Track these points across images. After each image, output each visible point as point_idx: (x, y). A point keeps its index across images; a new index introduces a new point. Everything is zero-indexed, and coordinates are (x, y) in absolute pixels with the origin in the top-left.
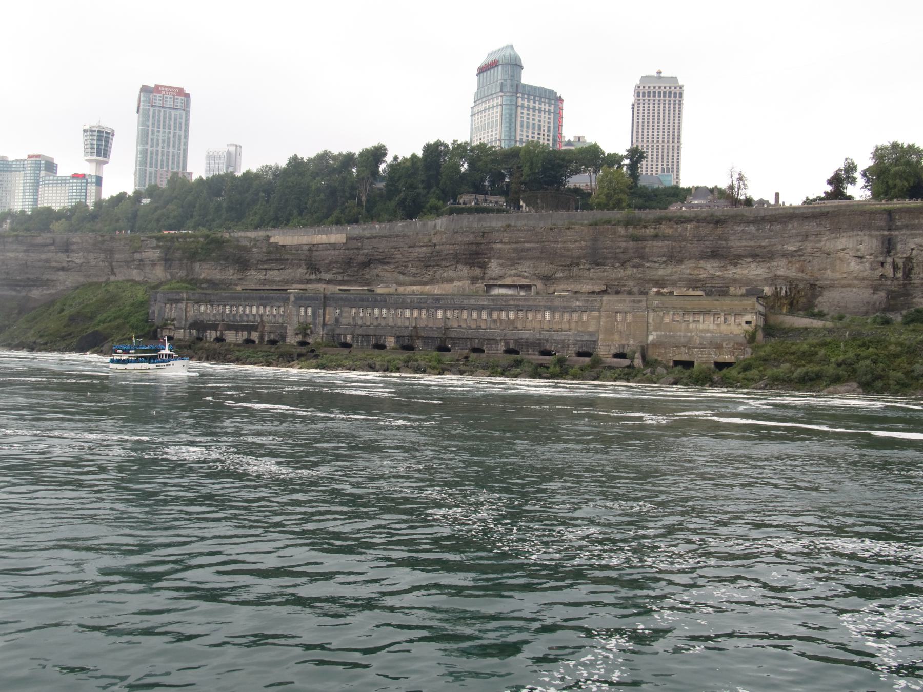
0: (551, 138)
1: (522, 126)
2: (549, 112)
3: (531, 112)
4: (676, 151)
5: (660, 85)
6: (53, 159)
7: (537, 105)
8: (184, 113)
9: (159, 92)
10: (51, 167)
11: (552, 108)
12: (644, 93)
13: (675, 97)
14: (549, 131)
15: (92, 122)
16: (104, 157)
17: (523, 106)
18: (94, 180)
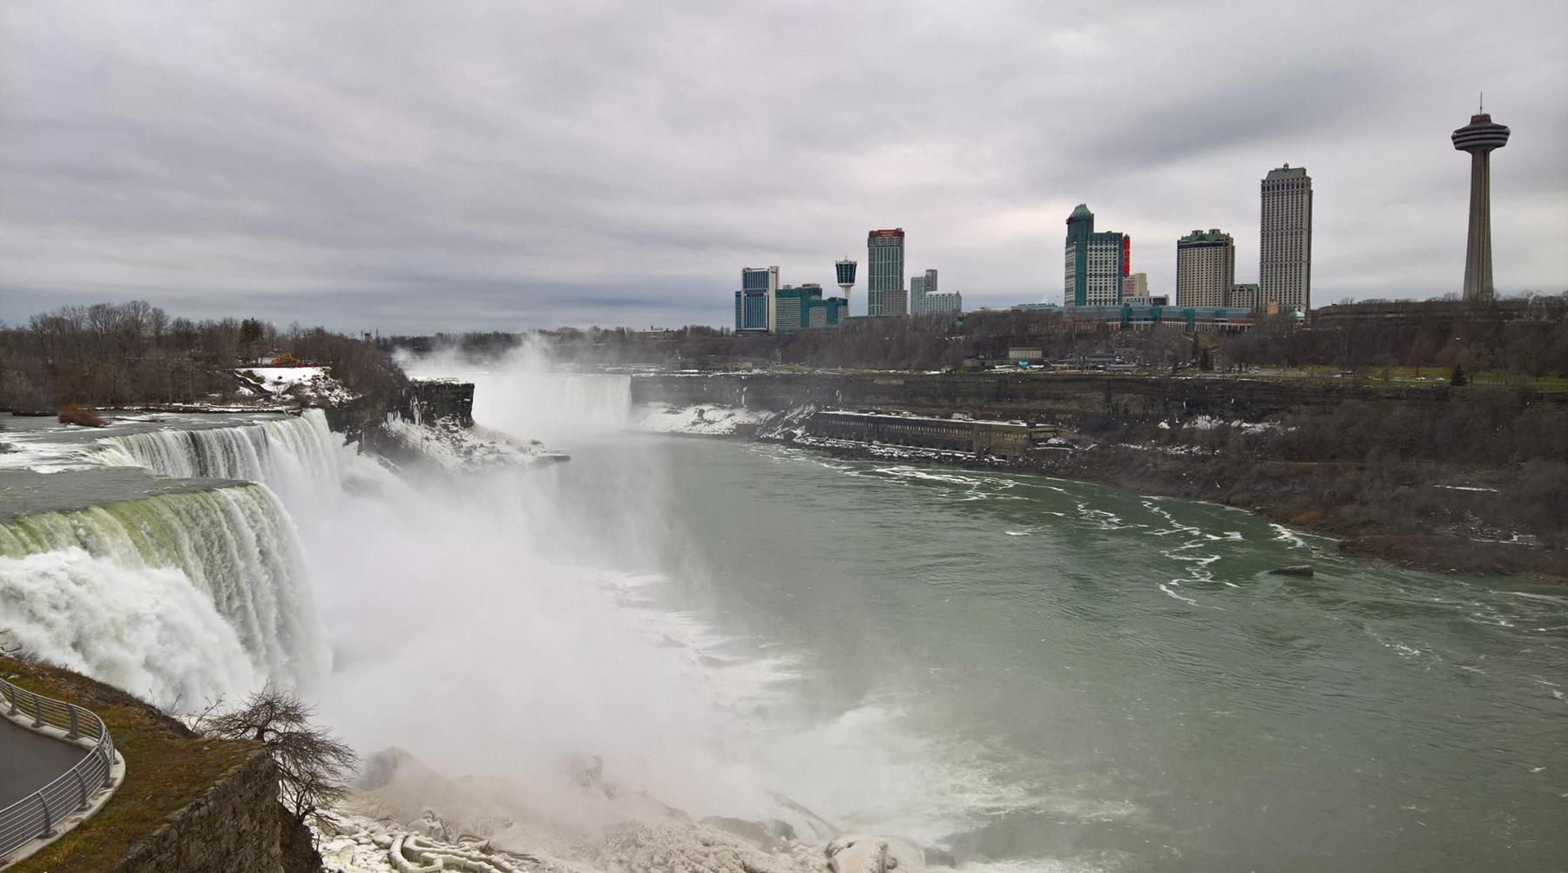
0: (1117, 269)
1: (1091, 264)
2: (1115, 250)
3: (1099, 253)
4: (1299, 236)
5: (1283, 178)
6: (819, 285)
7: (1104, 247)
8: (898, 248)
9: (881, 235)
10: (817, 291)
11: (1117, 247)
12: (1268, 187)
13: (1298, 187)
14: (1115, 264)
15: (841, 259)
16: (851, 282)
17: (1091, 250)
18: (841, 302)
